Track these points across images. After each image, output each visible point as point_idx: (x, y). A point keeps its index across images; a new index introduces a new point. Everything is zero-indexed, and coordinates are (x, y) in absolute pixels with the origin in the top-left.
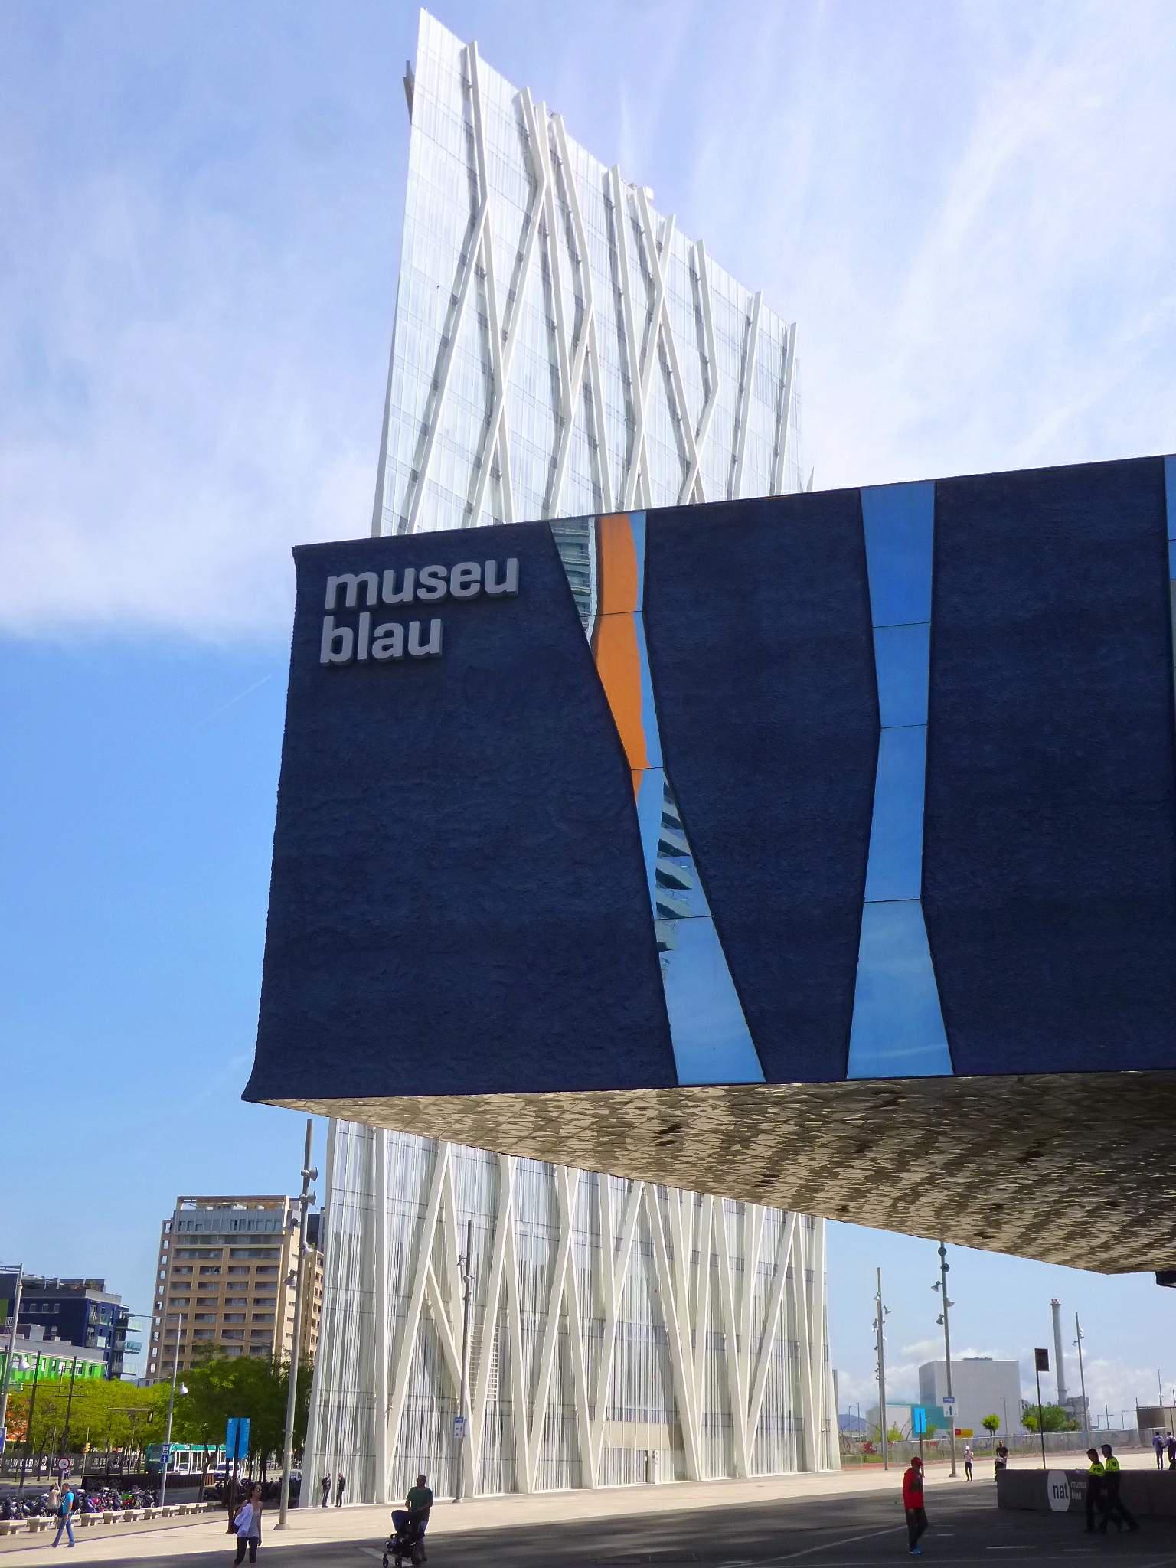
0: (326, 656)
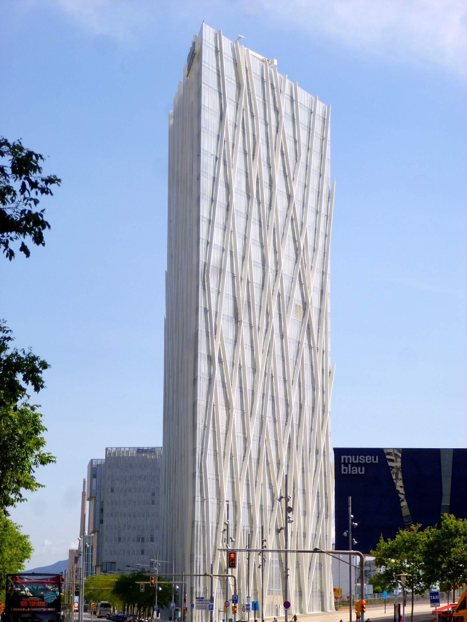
0: (343, 472)
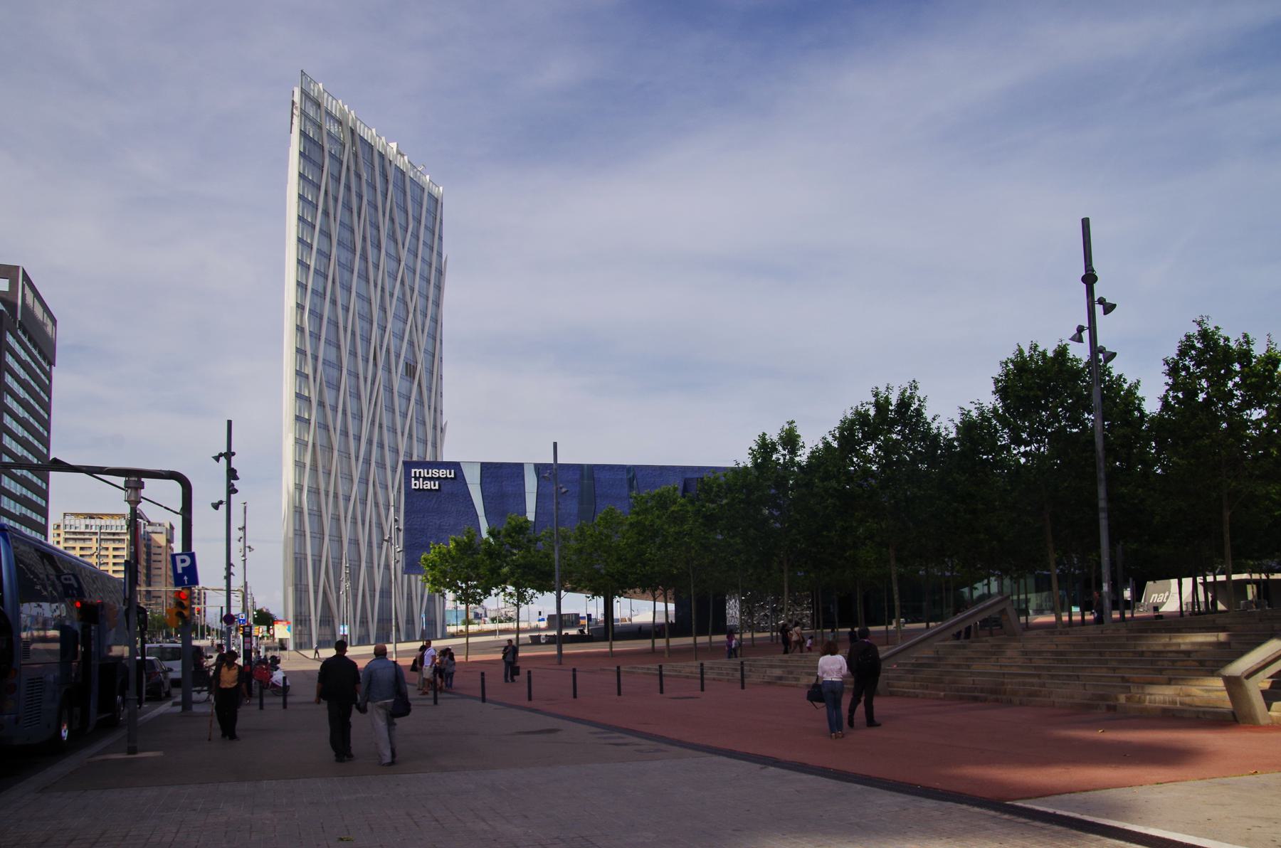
0: (413, 487)
